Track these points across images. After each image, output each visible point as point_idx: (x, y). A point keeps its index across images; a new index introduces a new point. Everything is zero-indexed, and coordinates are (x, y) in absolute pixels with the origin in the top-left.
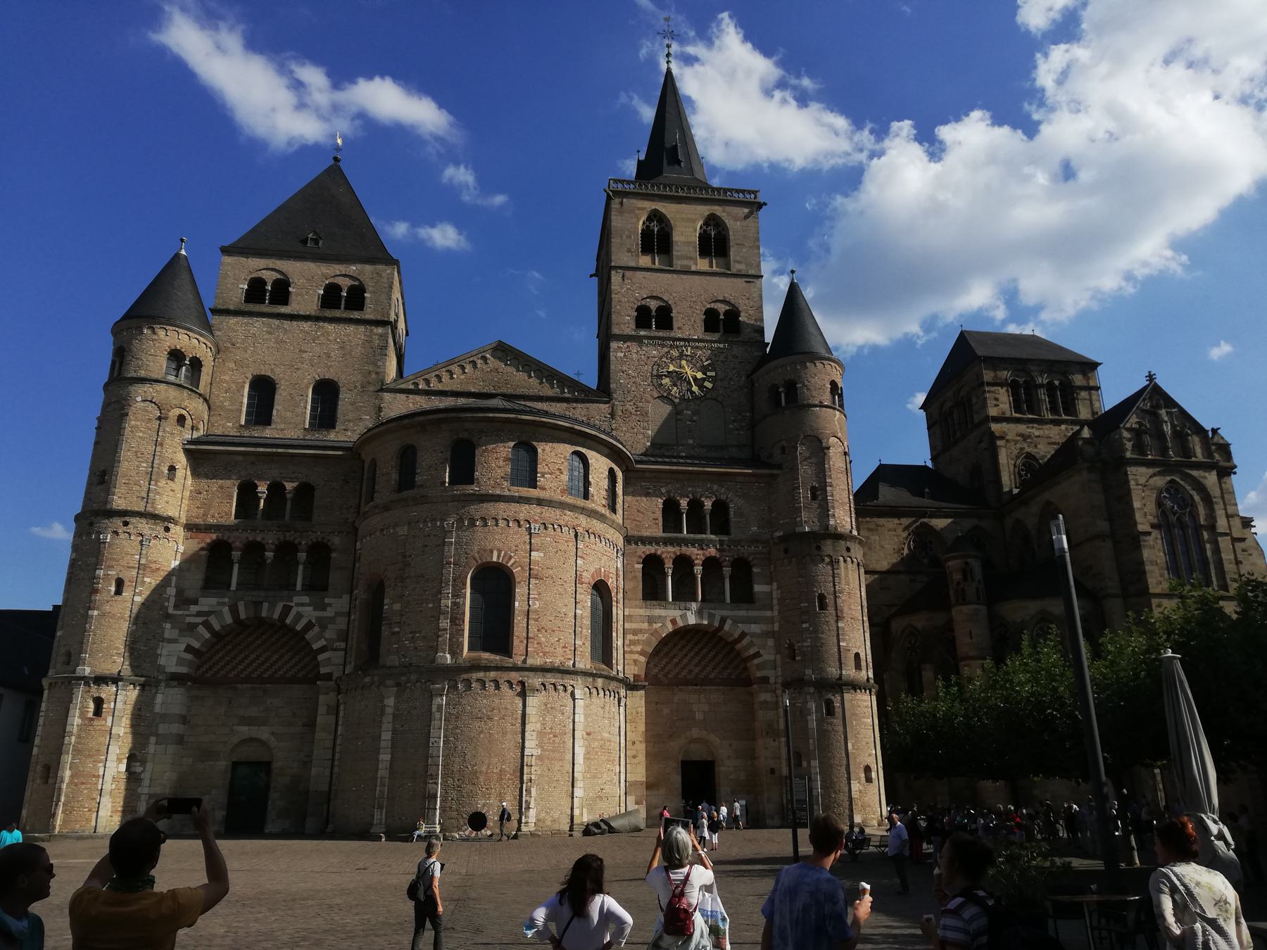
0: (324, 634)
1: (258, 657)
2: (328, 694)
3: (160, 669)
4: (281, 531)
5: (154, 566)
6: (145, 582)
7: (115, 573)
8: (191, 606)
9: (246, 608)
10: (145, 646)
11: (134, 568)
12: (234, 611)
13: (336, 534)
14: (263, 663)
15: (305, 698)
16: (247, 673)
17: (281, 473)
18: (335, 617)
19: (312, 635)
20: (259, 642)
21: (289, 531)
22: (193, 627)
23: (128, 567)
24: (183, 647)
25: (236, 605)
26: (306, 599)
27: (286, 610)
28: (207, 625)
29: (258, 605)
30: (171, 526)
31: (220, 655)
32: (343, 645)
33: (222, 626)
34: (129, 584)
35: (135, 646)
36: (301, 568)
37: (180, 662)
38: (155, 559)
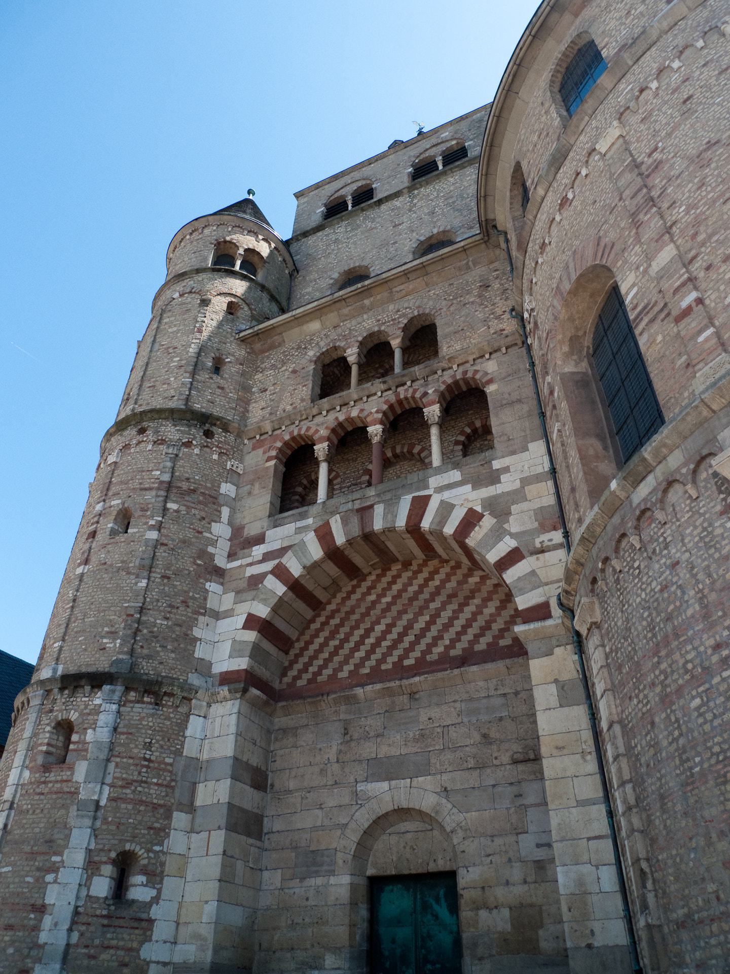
0: (506, 526)
1: (390, 627)
2: (550, 653)
3: (204, 668)
4: (390, 389)
5: (185, 486)
6: (168, 509)
7: (119, 501)
8: (254, 548)
9: (345, 522)
10: (167, 619)
11: (150, 489)
12: (324, 535)
13: (487, 356)
14: (401, 636)
15: (504, 695)
16: (373, 663)
17: (379, 320)
18: (523, 487)
19: (480, 536)
20: (388, 599)
21: (404, 384)
22: (256, 581)
23: (141, 489)
24: (241, 620)
25: (327, 524)
26: (455, 475)
27: (420, 505)
28: (280, 572)
29: (365, 512)
30: (217, 430)
31: (321, 640)
32: (557, 537)
33: (304, 567)
34: (141, 513)
35: (144, 618)
36: (434, 431)
37: (236, 652)
38: (187, 475)
